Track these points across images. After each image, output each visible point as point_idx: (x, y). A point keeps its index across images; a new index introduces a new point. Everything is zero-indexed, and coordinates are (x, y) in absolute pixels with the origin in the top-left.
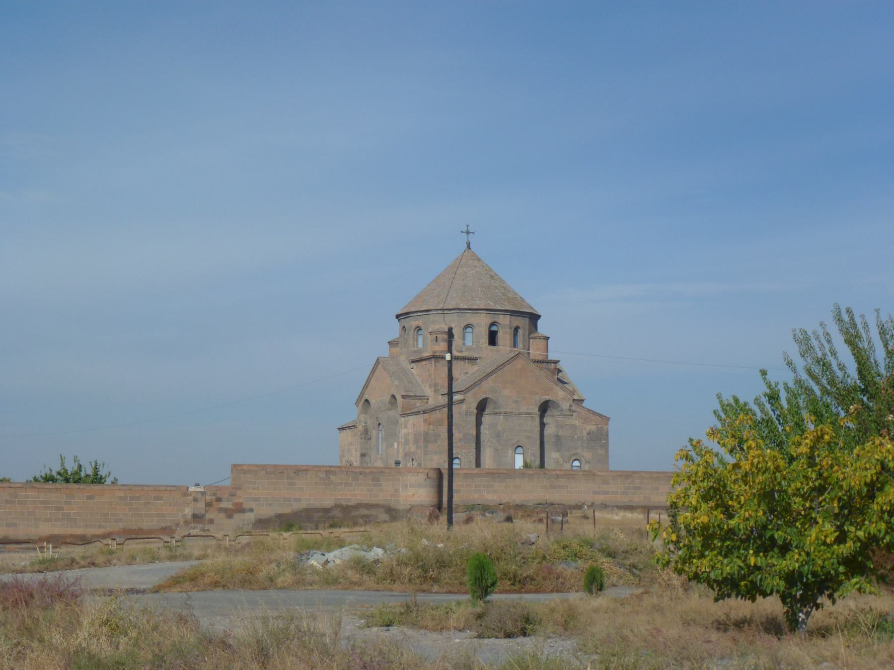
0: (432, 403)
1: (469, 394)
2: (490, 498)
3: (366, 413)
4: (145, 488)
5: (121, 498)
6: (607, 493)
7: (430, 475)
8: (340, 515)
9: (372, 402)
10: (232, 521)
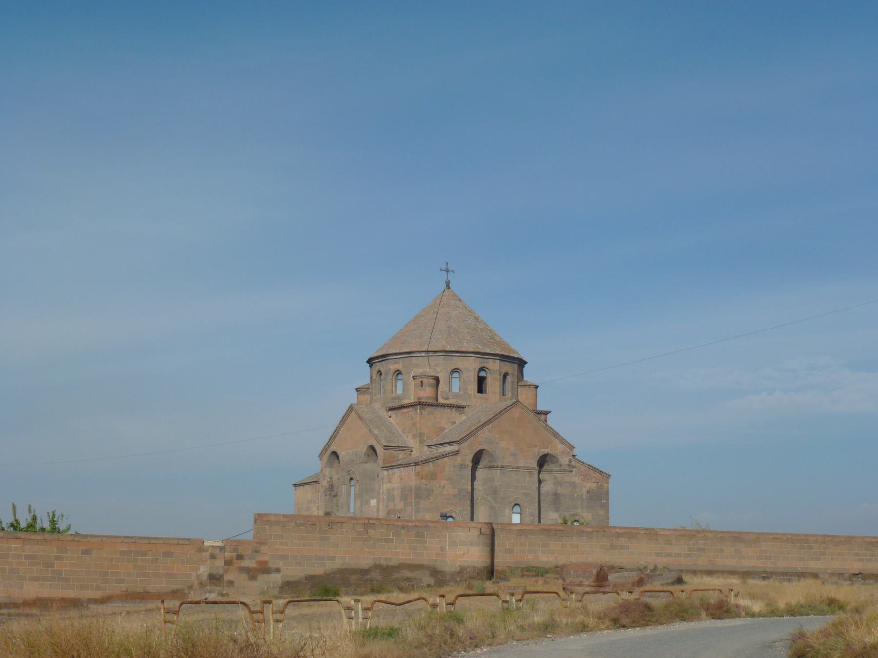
0: (416, 454)
1: (465, 445)
2: (545, 559)
3: (331, 467)
4: (153, 541)
5: (123, 553)
6: (669, 555)
7: (483, 530)
8: (380, 578)
9: (342, 454)
10: (255, 584)
